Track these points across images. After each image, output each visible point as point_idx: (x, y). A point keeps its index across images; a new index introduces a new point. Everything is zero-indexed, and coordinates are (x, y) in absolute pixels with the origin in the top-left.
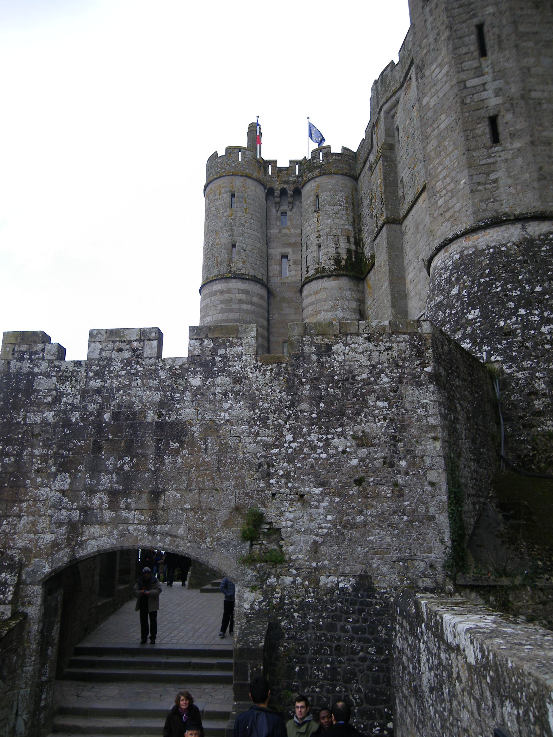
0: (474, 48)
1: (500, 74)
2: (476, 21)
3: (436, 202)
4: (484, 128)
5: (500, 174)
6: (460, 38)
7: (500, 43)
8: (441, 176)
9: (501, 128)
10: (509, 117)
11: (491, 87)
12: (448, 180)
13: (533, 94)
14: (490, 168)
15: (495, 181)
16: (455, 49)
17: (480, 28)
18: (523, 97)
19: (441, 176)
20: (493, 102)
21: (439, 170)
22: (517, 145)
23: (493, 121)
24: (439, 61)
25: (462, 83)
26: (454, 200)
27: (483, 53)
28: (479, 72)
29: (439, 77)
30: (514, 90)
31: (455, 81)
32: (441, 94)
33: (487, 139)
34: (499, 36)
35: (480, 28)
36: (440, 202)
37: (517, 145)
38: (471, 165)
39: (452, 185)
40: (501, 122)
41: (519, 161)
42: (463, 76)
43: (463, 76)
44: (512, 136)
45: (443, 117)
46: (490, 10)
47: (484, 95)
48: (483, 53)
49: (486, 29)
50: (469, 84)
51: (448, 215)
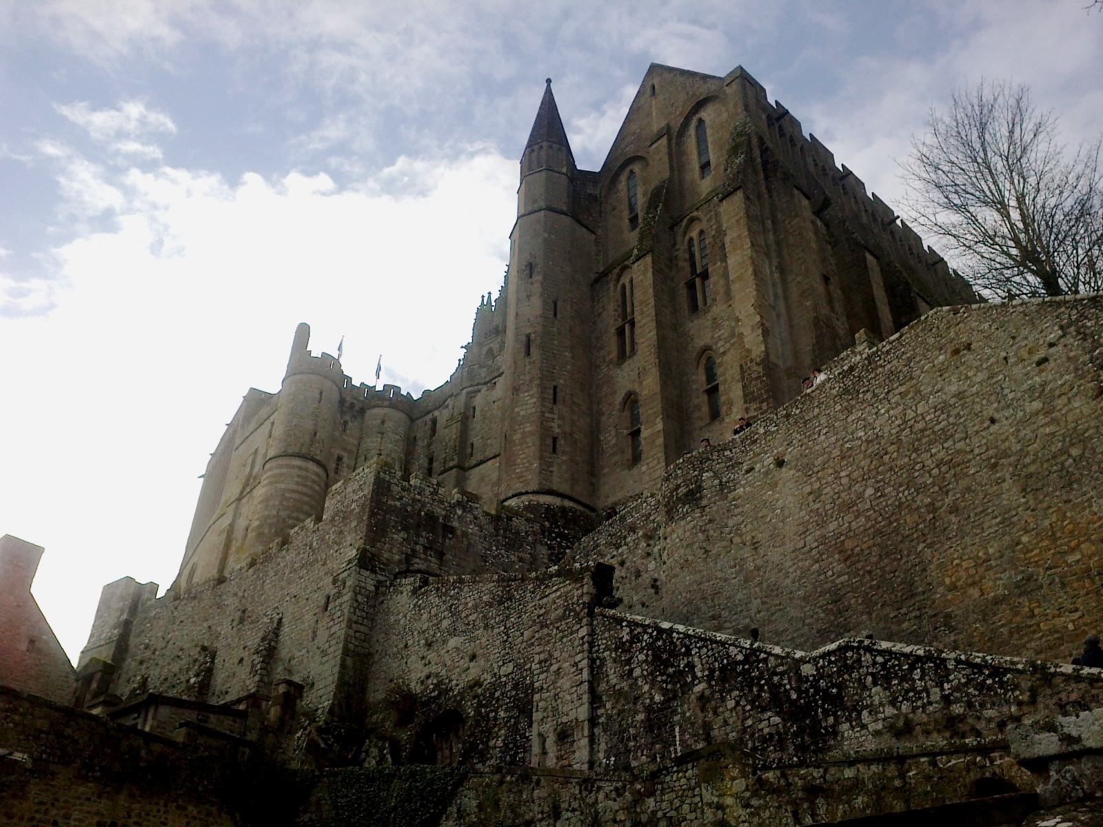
0: (551, 397)
1: (561, 417)
2: (554, 383)
3: (515, 469)
4: (549, 442)
5: (554, 469)
6: (546, 388)
7: (564, 401)
8: (521, 457)
9: (558, 446)
10: (562, 442)
11: (557, 422)
12: (525, 461)
13: (575, 436)
14: (550, 464)
15: (551, 472)
16: (542, 392)
17: (555, 388)
18: (570, 434)
19: (524, 456)
20: (557, 430)
21: (521, 452)
22: (564, 458)
23: (555, 440)
24: (531, 393)
25: (543, 413)
26: (528, 473)
27: (555, 403)
28: (551, 412)
29: (529, 402)
30: (567, 429)
31: (539, 410)
32: (529, 412)
33: (550, 449)
34: (564, 397)
35: (555, 388)
36: (518, 471)
37: (564, 458)
38: (541, 458)
39: (527, 465)
40: (558, 442)
41: (564, 467)
42: (544, 409)
43: (544, 409)
44: (563, 452)
45: (528, 425)
46: (562, 381)
47: (553, 424)
48: (555, 403)
49: (558, 390)
50: (546, 415)
51: (522, 479)
